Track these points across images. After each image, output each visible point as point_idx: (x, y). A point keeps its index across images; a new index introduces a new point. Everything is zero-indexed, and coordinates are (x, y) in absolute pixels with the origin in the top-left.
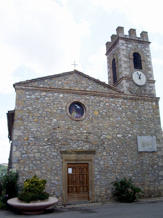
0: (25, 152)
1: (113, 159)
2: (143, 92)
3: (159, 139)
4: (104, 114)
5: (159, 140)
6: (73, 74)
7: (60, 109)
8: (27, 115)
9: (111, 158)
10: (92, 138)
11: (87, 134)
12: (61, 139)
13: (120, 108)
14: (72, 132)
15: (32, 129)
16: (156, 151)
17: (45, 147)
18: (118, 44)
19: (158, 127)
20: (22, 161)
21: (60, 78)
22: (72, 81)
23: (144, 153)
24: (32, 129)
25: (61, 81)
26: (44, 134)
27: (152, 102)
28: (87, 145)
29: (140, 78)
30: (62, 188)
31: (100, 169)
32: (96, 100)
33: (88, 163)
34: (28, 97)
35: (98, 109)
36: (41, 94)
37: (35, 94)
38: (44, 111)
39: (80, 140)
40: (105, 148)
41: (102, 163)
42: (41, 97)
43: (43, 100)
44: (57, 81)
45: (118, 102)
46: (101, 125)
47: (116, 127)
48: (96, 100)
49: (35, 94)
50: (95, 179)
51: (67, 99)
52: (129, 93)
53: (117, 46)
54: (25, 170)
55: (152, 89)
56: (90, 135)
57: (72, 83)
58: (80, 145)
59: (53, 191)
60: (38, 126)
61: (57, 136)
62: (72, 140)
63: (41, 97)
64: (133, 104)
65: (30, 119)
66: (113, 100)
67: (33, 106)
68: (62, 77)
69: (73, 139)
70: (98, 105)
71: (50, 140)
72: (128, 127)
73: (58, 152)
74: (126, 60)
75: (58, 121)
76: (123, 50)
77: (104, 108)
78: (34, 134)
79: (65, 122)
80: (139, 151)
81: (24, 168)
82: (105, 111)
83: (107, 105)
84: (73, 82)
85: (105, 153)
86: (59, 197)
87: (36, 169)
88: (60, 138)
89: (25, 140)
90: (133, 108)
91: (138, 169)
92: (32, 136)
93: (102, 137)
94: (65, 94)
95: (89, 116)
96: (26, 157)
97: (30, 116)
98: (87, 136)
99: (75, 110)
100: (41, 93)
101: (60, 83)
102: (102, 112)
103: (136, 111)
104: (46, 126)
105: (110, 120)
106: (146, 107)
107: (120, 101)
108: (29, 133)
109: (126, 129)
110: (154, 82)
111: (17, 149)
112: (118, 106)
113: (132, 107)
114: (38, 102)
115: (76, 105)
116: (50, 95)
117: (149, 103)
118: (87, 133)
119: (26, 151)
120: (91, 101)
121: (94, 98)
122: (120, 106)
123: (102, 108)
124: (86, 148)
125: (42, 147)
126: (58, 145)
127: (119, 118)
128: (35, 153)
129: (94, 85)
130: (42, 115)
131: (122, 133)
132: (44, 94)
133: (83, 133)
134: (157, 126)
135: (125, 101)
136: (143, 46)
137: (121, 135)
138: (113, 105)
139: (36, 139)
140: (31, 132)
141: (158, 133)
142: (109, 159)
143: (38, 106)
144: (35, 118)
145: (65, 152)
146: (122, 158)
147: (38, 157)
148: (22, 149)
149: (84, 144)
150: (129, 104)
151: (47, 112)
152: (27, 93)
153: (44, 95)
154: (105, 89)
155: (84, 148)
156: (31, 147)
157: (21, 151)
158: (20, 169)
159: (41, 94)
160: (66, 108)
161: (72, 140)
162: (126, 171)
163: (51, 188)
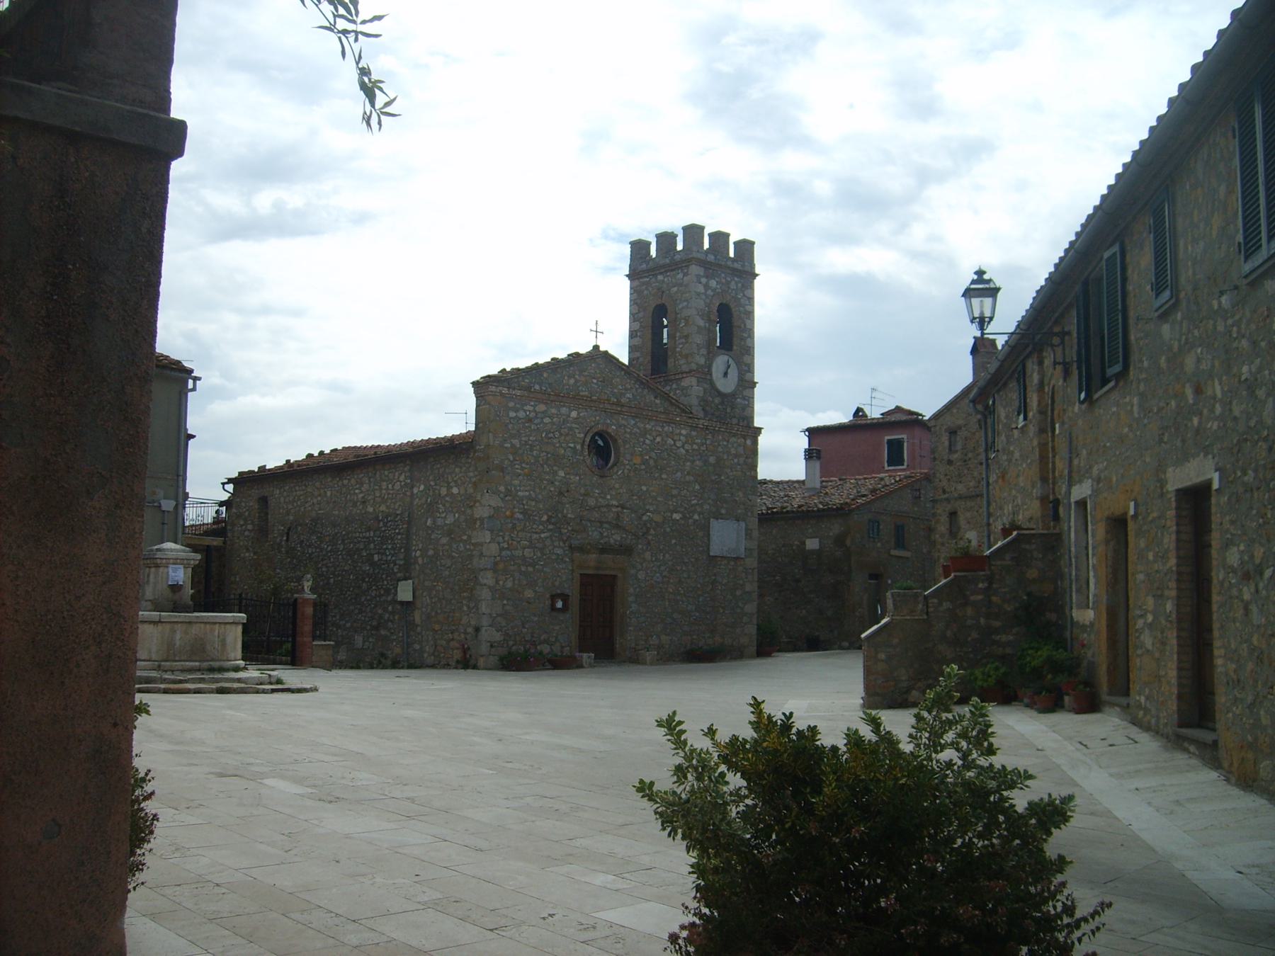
1: (663, 568)
2: (729, 410)
3: (751, 530)
4: (652, 462)
5: (749, 532)
6: (597, 360)
9: (659, 567)
11: (619, 509)
12: (570, 518)
13: (682, 450)
14: (591, 502)
16: (743, 556)
17: (542, 536)
18: (685, 274)
19: (750, 501)
20: (501, 566)
21: (572, 368)
22: (594, 378)
23: (719, 559)
25: (574, 377)
26: (541, 506)
27: (744, 437)
28: (618, 534)
29: (726, 374)
31: (638, 590)
33: (614, 577)
34: (512, 414)
35: (641, 449)
36: (537, 409)
37: (525, 408)
38: (543, 452)
40: (649, 543)
41: (641, 575)
42: (536, 417)
43: (539, 424)
44: (566, 378)
45: (680, 434)
46: (644, 488)
47: (673, 496)
49: (525, 408)
50: (628, 612)
52: (701, 415)
53: (680, 276)
55: (747, 403)
56: (625, 511)
58: (605, 534)
60: (530, 485)
61: (565, 511)
62: (590, 521)
63: (536, 417)
64: (708, 442)
65: (517, 469)
66: (671, 428)
68: (576, 368)
69: (593, 519)
70: (642, 440)
71: (553, 520)
72: (693, 498)
74: (701, 323)
75: (568, 476)
76: (698, 294)
78: (523, 505)
79: (580, 479)
80: (712, 554)
83: (659, 442)
84: (595, 381)
85: (648, 555)
87: (527, 584)
88: (569, 516)
90: (706, 452)
91: (706, 595)
92: (519, 509)
93: (645, 518)
94: (580, 410)
95: (622, 467)
99: (594, 448)
100: (536, 405)
101: (572, 381)
102: (647, 457)
103: (712, 460)
105: (662, 479)
106: (733, 451)
107: (684, 432)
109: (690, 501)
110: (754, 384)
111: (492, 538)
112: (678, 445)
113: (703, 448)
114: (531, 427)
116: (554, 411)
117: (739, 441)
118: (617, 507)
122: (683, 447)
123: (648, 447)
124: (616, 541)
125: (537, 536)
127: (679, 474)
128: (525, 548)
129: (637, 389)
131: (682, 510)
132: (541, 408)
133: (612, 505)
134: (750, 497)
135: (694, 433)
136: (740, 285)
137: (680, 515)
138: (670, 441)
141: (749, 514)
142: (654, 569)
143: (531, 438)
145: (581, 549)
146: (679, 568)
147: (530, 558)
149: (613, 532)
150: (699, 441)
151: (548, 453)
152: (511, 404)
153: (543, 412)
154: (656, 401)
155: (612, 541)
156: (517, 535)
157: (499, 543)
159: (537, 409)
160: (583, 445)
161: (590, 521)
162: (684, 599)
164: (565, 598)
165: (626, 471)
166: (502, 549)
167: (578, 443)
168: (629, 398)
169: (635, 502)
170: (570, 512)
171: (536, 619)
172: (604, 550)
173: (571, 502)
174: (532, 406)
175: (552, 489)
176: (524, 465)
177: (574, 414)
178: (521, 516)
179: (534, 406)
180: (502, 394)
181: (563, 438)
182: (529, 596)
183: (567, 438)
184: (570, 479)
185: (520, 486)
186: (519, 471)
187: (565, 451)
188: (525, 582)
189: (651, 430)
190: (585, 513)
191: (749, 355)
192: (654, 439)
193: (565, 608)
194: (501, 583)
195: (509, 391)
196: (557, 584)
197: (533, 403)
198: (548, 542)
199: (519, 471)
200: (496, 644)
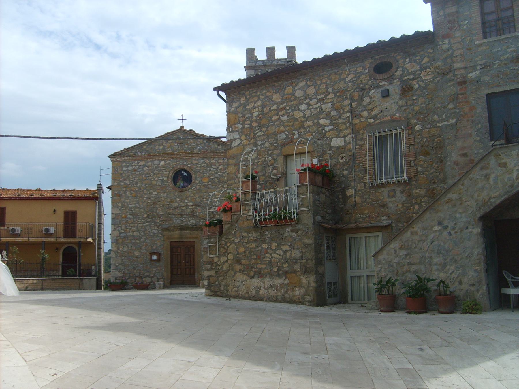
0: (123, 231)
4: (216, 180)
6: (177, 134)
7: (160, 180)
8: (124, 189)
10: (199, 212)
11: (194, 207)
12: (161, 214)
14: (175, 205)
15: (130, 206)
17: (145, 225)
20: (121, 241)
22: (175, 143)
24: (130, 206)
30: (163, 270)
32: (206, 163)
34: (125, 169)
36: (139, 164)
39: (185, 215)
42: (139, 168)
44: (157, 146)
48: (206, 163)
51: (169, 167)
54: (124, 250)
56: (197, 207)
57: (176, 146)
58: (185, 220)
59: (153, 273)
60: (136, 201)
61: (158, 212)
62: (174, 215)
63: (139, 168)
67: (131, 180)
70: (209, 169)
71: (150, 217)
73: (159, 230)
75: (159, 194)
77: (217, 173)
79: (167, 195)
81: (123, 248)
82: (217, 176)
83: (221, 169)
84: (176, 144)
86: (160, 279)
88: (161, 213)
89: (123, 218)
92: (130, 213)
95: (195, 185)
96: (124, 236)
97: (127, 191)
98: (193, 209)
99: (181, 178)
101: (161, 147)
102: (213, 178)
104: (145, 201)
108: (127, 210)
111: (115, 228)
114: (135, 173)
115: (182, 172)
116: (150, 163)
118: (192, 206)
119: (124, 230)
120: (199, 165)
121: (204, 161)
124: (192, 223)
125: (141, 225)
126: (159, 221)
129: (205, 143)
130: (141, 189)
132: (142, 163)
133: (189, 205)
139: (135, 216)
140: (128, 208)
143: (136, 179)
144: (133, 192)
145: (167, 229)
147: (137, 236)
148: (120, 228)
149: (190, 219)
151: (146, 184)
152: (124, 164)
154: (219, 147)
155: (189, 224)
156: (129, 226)
157: (119, 230)
158: (119, 250)
159: (139, 164)
161: (174, 215)
163: (151, 269)
164: (159, 255)
165: (198, 187)
166: (120, 233)
167: (165, 177)
168: (199, 149)
169: (205, 202)
170: (161, 211)
171: (141, 265)
172: (182, 229)
173: (161, 207)
174: (136, 163)
175: (149, 201)
176: (132, 192)
177: (162, 163)
178: (131, 216)
179: (138, 163)
180: (117, 161)
181: (155, 175)
182: (137, 254)
183: (158, 176)
184: (160, 195)
185: (130, 202)
186: (129, 195)
187: (157, 182)
188: (135, 248)
189: (215, 163)
190: (171, 211)
192: (218, 168)
193: (158, 260)
194: (121, 249)
195: (121, 158)
196: (154, 247)
197: (136, 162)
198: (148, 228)
199: (129, 195)
200: (118, 278)
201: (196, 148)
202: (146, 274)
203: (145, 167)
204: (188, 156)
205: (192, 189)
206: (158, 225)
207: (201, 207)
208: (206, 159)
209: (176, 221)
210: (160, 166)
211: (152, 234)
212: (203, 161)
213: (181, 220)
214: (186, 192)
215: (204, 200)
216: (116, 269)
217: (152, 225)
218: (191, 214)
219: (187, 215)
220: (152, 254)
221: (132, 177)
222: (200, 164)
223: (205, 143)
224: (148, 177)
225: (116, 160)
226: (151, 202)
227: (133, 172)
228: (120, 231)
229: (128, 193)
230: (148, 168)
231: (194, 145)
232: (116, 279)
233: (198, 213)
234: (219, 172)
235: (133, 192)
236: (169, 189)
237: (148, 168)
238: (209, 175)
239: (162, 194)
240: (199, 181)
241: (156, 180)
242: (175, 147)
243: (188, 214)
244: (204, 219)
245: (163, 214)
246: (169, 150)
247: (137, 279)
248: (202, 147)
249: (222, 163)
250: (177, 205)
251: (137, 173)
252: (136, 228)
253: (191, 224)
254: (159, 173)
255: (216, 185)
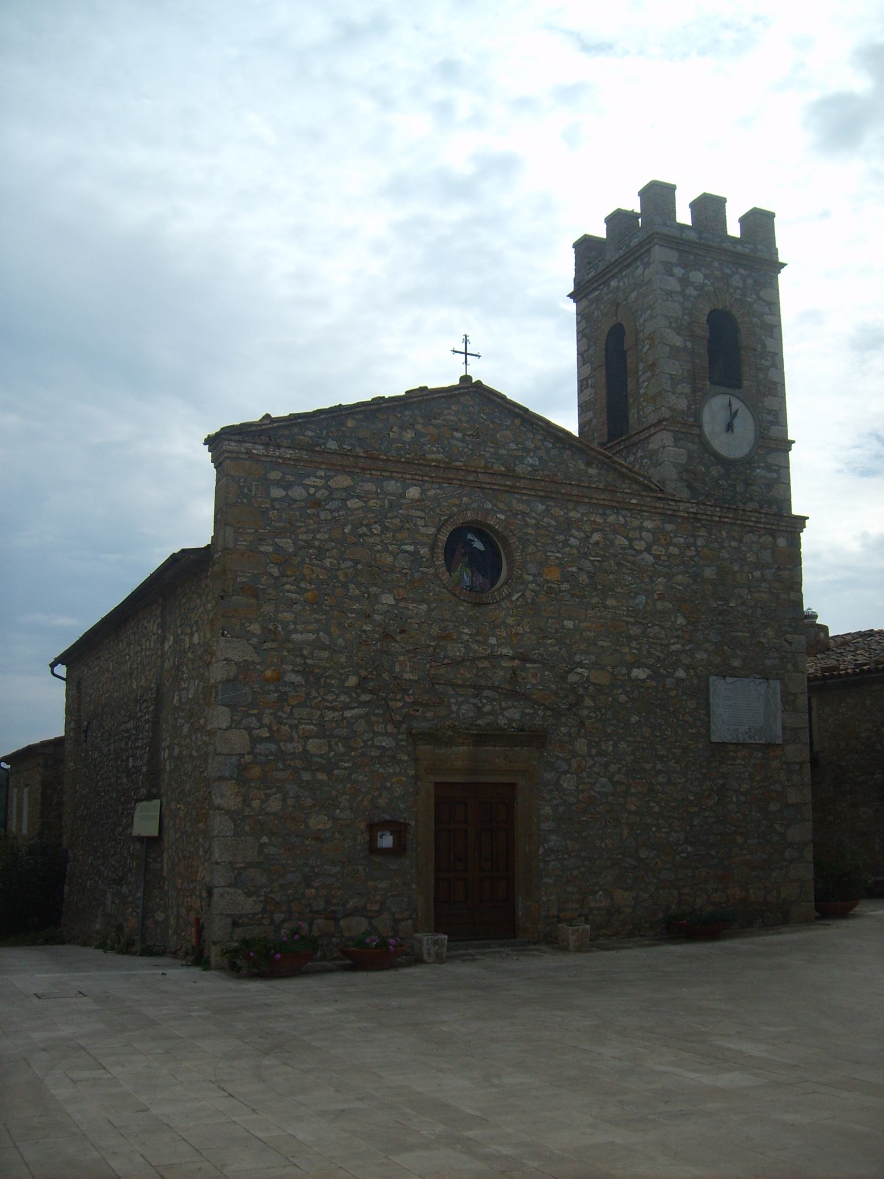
0: (268, 735)
1: (613, 768)
2: (740, 488)
3: (795, 694)
4: (583, 578)
5: (792, 698)
6: (462, 399)
7: (407, 552)
8: (275, 571)
9: (606, 766)
10: (534, 681)
11: (516, 662)
12: (410, 680)
13: (646, 556)
14: (456, 651)
15: (296, 637)
16: (779, 741)
17: (348, 714)
18: (646, 266)
19: (790, 643)
20: (256, 771)
21: (407, 413)
22: (456, 430)
23: (732, 748)
24: (296, 637)
25: (412, 426)
26: (343, 660)
27: (773, 534)
28: (516, 707)
29: (730, 427)
30: (414, 886)
31: (561, 809)
32: (553, 517)
33: (513, 786)
34: (277, 492)
35: (559, 555)
36: (331, 483)
37: (307, 481)
38: (345, 560)
39: (489, 688)
40: (582, 724)
41: (568, 783)
42: (330, 498)
43: (337, 510)
44: (395, 429)
45: (641, 528)
46: (569, 624)
47: (630, 638)
48: (553, 517)
49: (307, 481)
50: (541, 851)
51: (438, 511)
52: (685, 494)
53: (639, 271)
54: (268, 810)
55: (775, 475)
56: (527, 665)
57: (458, 439)
58: (487, 708)
59: (378, 898)
60: (318, 621)
61: (397, 668)
62: (453, 685)
63: (330, 498)
64: (700, 542)
65: (288, 591)
66: (621, 518)
67: (300, 537)
68: (416, 412)
69: (460, 682)
70: (562, 538)
72: (672, 641)
73: (399, 737)
74: (678, 341)
75: (402, 604)
76: (670, 293)
77: (585, 556)
78: (304, 657)
79: (430, 610)
80: (714, 738)
81: (263, 802)
82: (586, 564)
83: (597, 543)
84: (459, 435)
85: (581, 746)
86: (403, 920)
87: (314, 805)
88: (407, 676)
89: (267, 681)
90: (697, 559)
91: (707, 814)
93: (572, 678)
94: (427, 486)
95: (522, 587)
96: (271, 753)
97: (285, 580)
98: (514, 671)
100: (331, 477)
101: (409, 435)
102: (574, 569)
103: (709, 572)
104: (351, 625)
105: (606, 607)
106: (751, 557)
107: (648, 524)
108: (285, 653)
109: (667, 646)
110: (787, 445)
111: (233, 721)
112: (637, 548)
113: (692, 552)
114: (318, 516)
115: (470, 536)
116: (369, 487)
117: (761, 540)
118: (512, 658)
119: (270, 730)
120: (533, 522)
121: (546, 510)
122: (648, 550)
123: (575, 551)
124: (511, 720)
125: (337, 714)
126: (400, 704)
127: (642, 599)
128: (308, 738)
129: (548, 451)
130: (336, 577)
131: (651, 661)
132: (342, 481)
133: (501, 656)
134: (789, 637)
135: (669, 527)
136: (750, 281)
137: (648, 671)
138: (621, 541)
139: (311, 679)
140: (290, 646)
141: (789, 666)
142: (596, 770)
143: (318, 536)
144: (308, 586)
145: (433, 737)
146: (648, 766)
147: (321, 756)
148: (254, 722)
149: (504, 704)
150: (682, 540)
151: (357, 562)
152: (275, 475)
153: (345, 489)
154: (590, 471)
155: (502, 721)
156: (291, 713)
157: (249, 730)
158: (249, 806)
159: (331, 483)
160: (433, 547)
161: (453, 685)
162: (661, 821)
163: (370, 883)
164: (399, 829)
165: (528, 594)
166: (256, 741)
167: (423, 544)
168: (531, 465)
169: (551, 649)
170: (408, 669)
171: (335, 870)
172: (481, 738)
173: (408, 651)
174: (321, 477)
175: (367, 628)
176: (302, 585)
177: (413, 492)
178: (298, 679)
179: (328, 478)
180: (251, 456)
181: (389, 535)
182: (320, 827)
183: (399, 536)
184: (407, 608)
185: (295, 623)
186: (294, 596)
187: (395, 559)
188: (309, 802)
189: (581, 520)
190: (442, 671)
191: (776, 395)
192: (588, 537)
193: (399, 849)
194: (256, 804)
195: (267, 450)
196: (382, 802)
197: (322, 473)
198: (361, 726)
199: (294, 596)
200: (246, 920)
201: (521, 459)
202: (351, 904)
203: (353, 497)
204: (502, 482)
205: (512, 602)
206: (398, 718)
207: (540, 665)
208: (552, 504)
209: (459, 709)
210: (405, 501)
211: (374, 753)
212: (544, 507)
213: (474, 704)
214: (491, 607)
215: (549, 641)
216: (234, 885)
217: (374, 718)
218: (508, 687)
219: (493, 688)
220: (374, 828)
221: (304, 529)
222: (534, 518)
223: (548, 451)
224: (361, 536)
225: (248, 452)
226: (374, 631)
227: (309, 511)
228: (256, 732)
229: (287, 587)
230: (361, 504)
231: (515, 447)
232: (235, 924)
233: (529, 686)
234: (593, 553)
235: (308, 586)
236: (437, 589)
237: (361, 504)
238: (562, 559)
239: (411, 606)
240: (534, 576)
241: (391, 553)
242: (453, 442)
243: (498, 687)
244: (550, 709)
245: (416, 678)
246: (435, 449)
247: (320, 921)
248: (540, 458)
249: (600, 524)
250: (463, 650)
251: (323, 515)
252: (315, 725)
253: (506, 722)
254: (400, 529)
255: (584, 597)
